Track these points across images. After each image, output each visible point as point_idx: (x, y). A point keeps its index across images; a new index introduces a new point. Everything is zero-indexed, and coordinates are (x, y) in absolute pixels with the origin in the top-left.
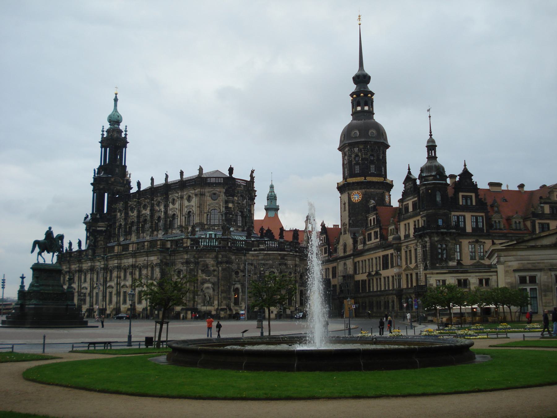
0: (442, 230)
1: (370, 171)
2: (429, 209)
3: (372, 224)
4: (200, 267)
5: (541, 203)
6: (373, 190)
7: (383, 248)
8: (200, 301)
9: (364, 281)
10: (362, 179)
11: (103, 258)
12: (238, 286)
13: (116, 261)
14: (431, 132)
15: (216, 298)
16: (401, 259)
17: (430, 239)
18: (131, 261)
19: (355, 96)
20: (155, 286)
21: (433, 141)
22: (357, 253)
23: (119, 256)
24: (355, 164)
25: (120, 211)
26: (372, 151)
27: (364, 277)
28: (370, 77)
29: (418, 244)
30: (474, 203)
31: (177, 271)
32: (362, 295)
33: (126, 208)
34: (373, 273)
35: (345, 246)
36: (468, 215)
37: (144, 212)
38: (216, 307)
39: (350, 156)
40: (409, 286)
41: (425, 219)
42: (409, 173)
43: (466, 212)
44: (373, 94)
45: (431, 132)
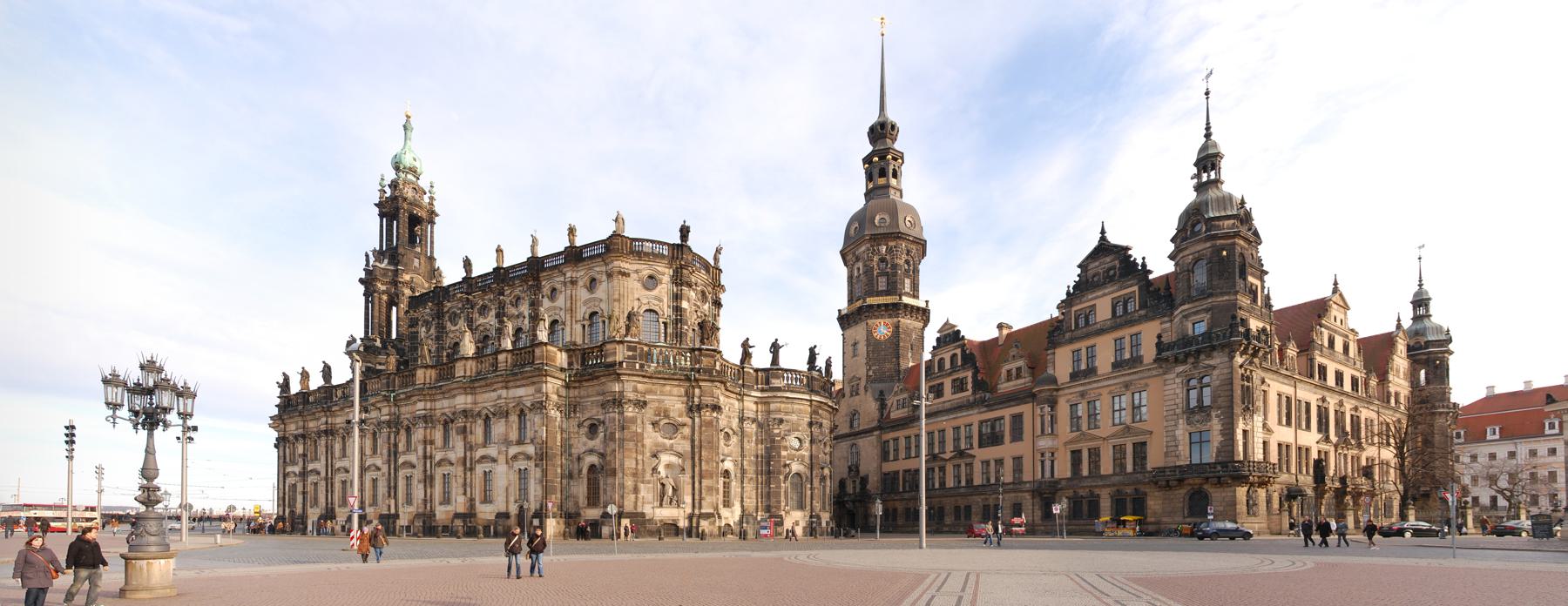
3: (948, 365)
4: (649, 413)
8: (650, 497)
11: (386, 399)
12: (728, 465)
13: (420, 405)
15: (688, 489)
18: (462, 401)
20: (529, 458)
23: (431, 391)
24: (879, 275)
25: (426, 323)
26: (908, 252)
31: (587, 424)
33: (439, 315)
37: (482, 321)
38: (689, 510)
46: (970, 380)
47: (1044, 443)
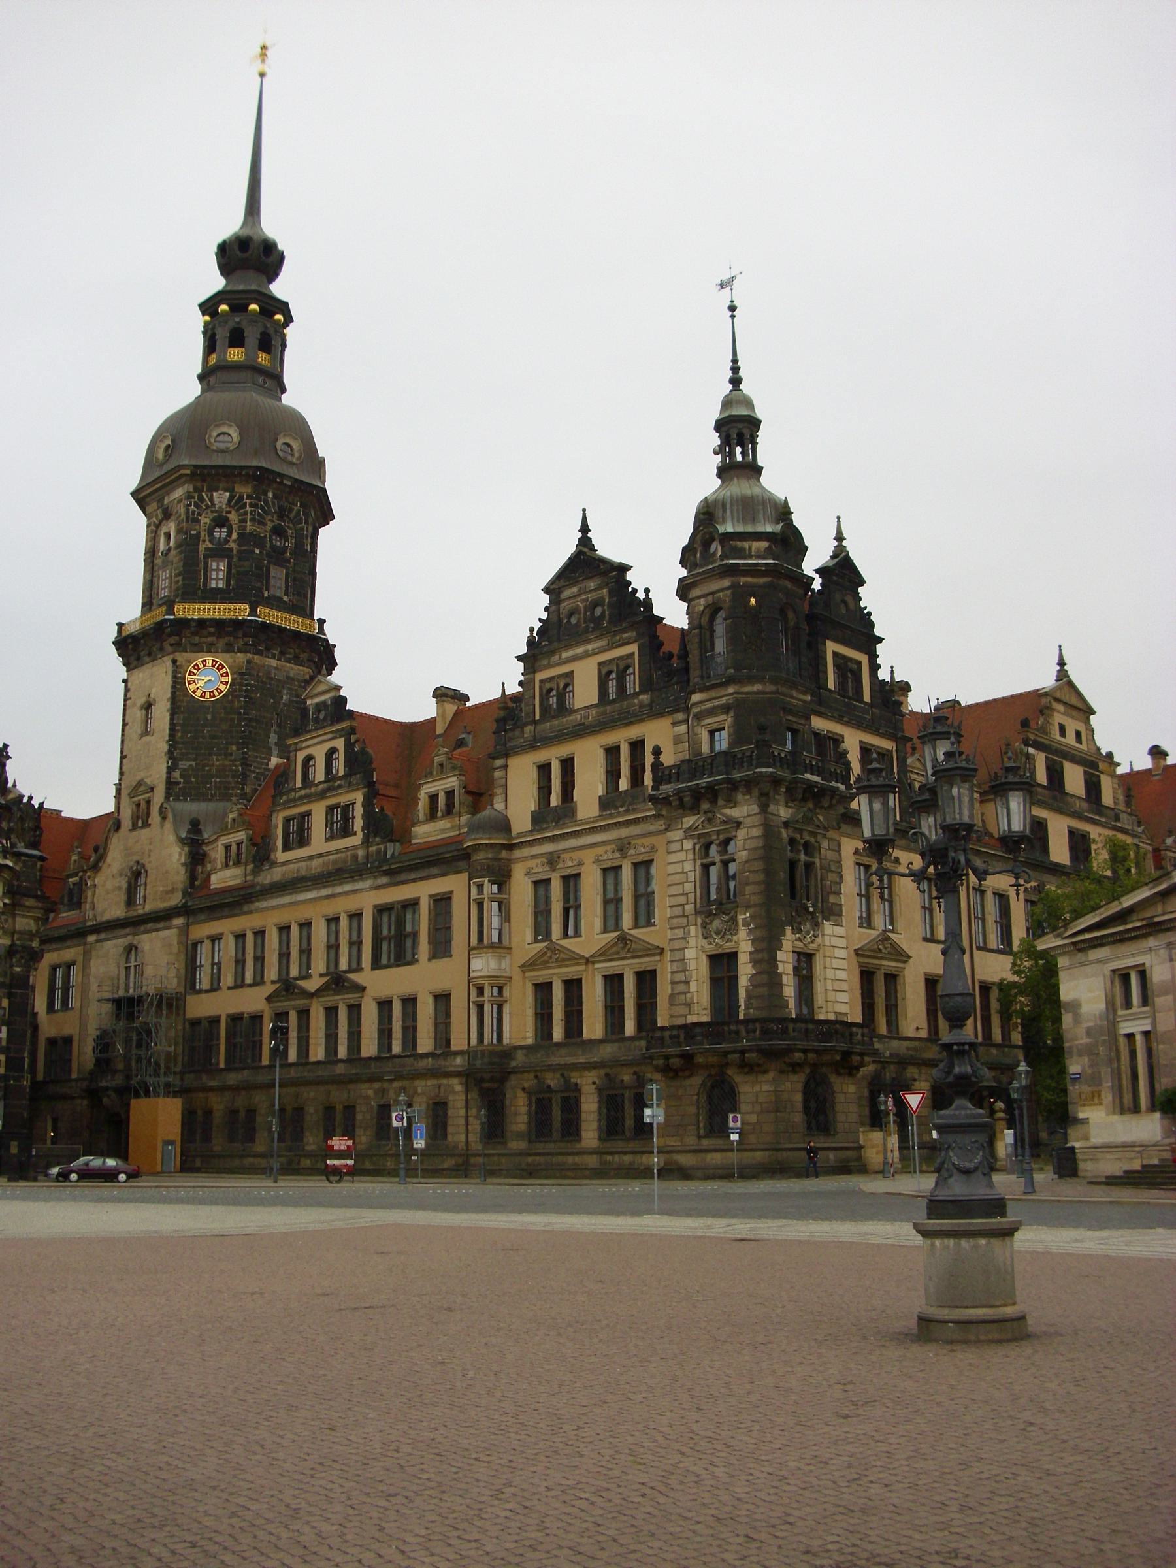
0: (808, 776)
1: (268, 589)
2: (751, 680)
3: (319, 773)
5: (1027, 745)
6: (274, 663)
7: (386, 873)
9: (245, 1026)
10: (242, 611)
14: (735, 369)
16: (506, 916)
17: (764, 808)
19: (224, 307)
21: (748, 403)
22: (200, 902)
26: (281, 514)
27: (253, 1001)
28: (281, 258)
29: (679, 834)
30: (867, 698)
32: (232, 1078)
34: (312, 985)
35: (136, 874)
36: (852, 740)
39: (192, 519)
40: (558, 1034)
41: (728, 720)
42: (585, 542)
43: (847, 723)
44: (289, 319)
45: (735, 369)
46: (359, 811)
47: (483, 965)
